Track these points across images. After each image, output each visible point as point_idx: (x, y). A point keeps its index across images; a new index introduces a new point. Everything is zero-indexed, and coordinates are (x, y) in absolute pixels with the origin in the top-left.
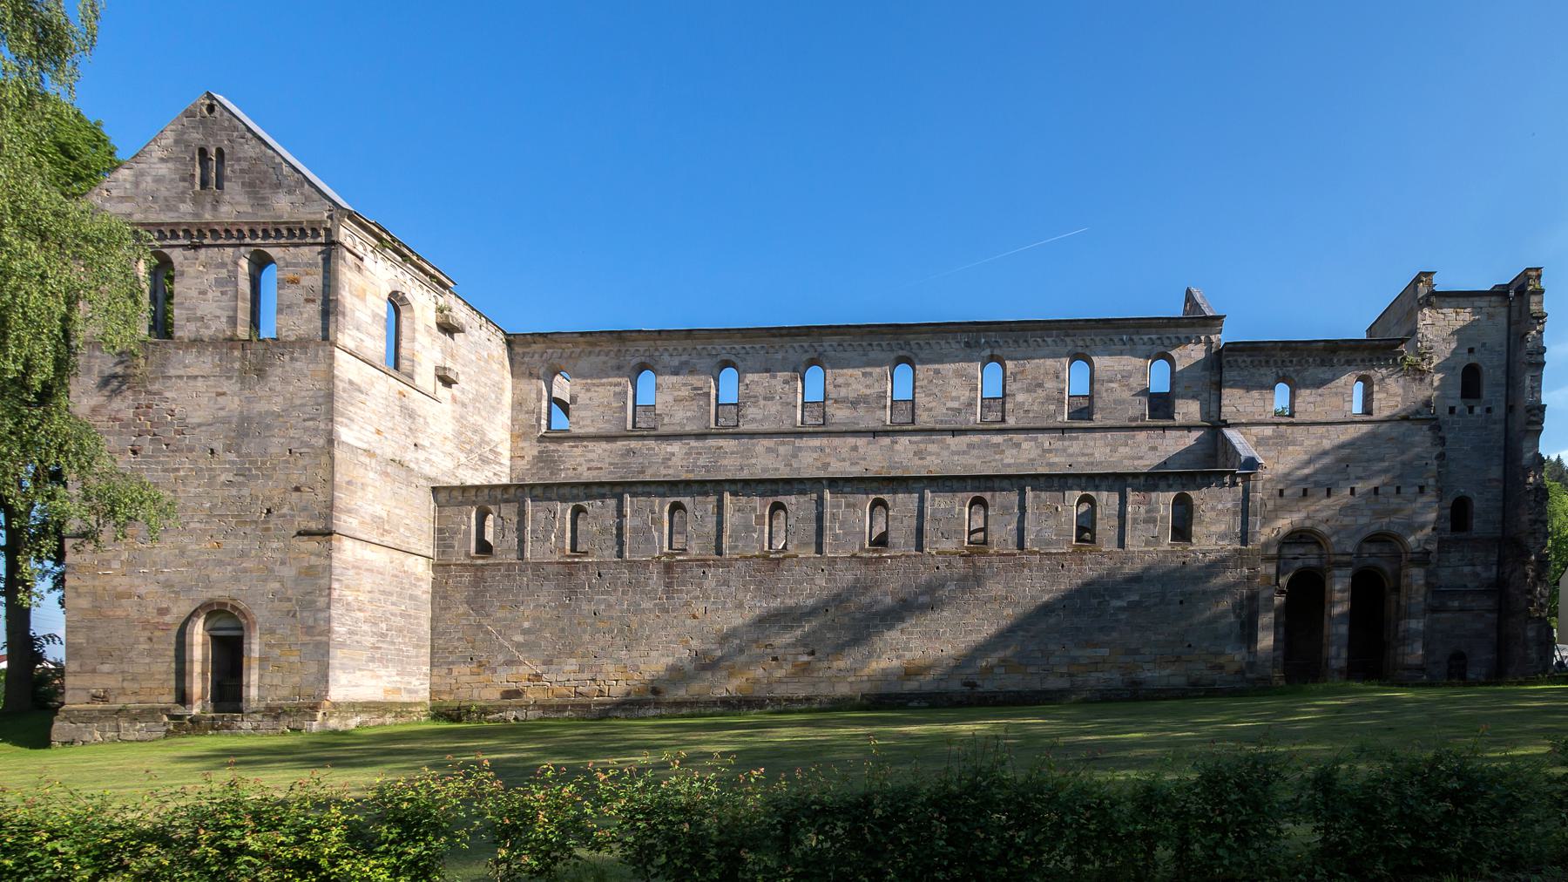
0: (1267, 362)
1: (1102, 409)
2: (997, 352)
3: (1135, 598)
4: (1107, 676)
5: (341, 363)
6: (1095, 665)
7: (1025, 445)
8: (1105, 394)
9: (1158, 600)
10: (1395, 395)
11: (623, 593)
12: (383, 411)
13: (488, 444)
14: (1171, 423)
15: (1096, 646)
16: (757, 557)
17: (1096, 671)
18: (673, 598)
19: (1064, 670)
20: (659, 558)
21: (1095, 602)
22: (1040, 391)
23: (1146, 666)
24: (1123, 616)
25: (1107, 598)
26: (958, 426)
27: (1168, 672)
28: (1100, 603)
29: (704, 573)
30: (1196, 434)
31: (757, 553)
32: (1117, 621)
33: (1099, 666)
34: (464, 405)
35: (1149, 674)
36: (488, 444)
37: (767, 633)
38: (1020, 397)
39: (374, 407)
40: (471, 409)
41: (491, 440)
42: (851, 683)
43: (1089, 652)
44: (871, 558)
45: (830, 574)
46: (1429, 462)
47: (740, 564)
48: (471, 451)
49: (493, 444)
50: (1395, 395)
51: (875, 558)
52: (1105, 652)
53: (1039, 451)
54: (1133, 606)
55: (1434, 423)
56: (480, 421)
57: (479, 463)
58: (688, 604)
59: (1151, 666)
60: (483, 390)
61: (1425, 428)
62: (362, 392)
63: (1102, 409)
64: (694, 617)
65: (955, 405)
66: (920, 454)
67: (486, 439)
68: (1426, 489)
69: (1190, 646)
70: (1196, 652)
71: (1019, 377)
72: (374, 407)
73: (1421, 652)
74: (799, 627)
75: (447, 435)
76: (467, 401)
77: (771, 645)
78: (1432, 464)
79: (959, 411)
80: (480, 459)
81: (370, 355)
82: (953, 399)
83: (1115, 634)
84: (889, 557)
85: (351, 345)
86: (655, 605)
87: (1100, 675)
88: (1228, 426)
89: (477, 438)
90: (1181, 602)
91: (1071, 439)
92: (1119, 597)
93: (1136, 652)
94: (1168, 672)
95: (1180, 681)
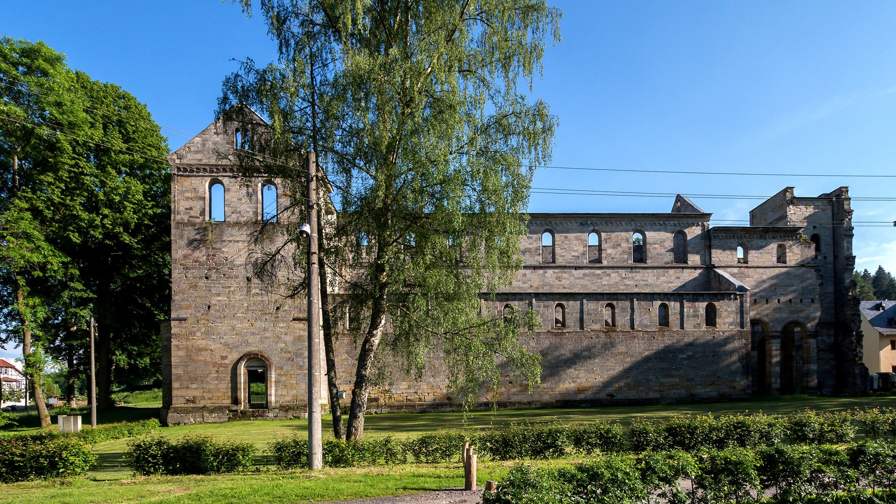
0: (734, 236)
1: (651, 258)
2: (596, 228)
3: (690, 353)
4: (678, 391)
7: (613, 275)
8: (652, 250)
14: (686, 265)
15: (672, 377)
19: (657, 388)
21: (671, 355)
22: (619, 248)
23: (697, 387)
24: (685, 362)
26: (578, 265)
30: (699, 271)
38: (609, 251)
43: (669, 380)
52: (677, 380)
53: (620, 278)
59: (700, 387)
63: (651, 258)
65: (576, 254)
66: (559, 279)
71: (608, 241)
73: (816, 381)
79: (578, 257)
82: (575, 251)
83: (682, 372)
87: (675, 391)
88: (716, 267)
91: (636, 272)
92: (683, 353)
93: (692, 380)
95: (714, 394)
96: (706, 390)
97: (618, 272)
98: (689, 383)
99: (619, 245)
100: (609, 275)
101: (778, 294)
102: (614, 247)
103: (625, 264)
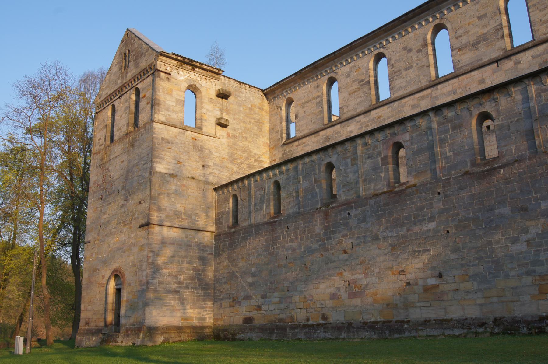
5: (157, 129)
11: (301, 240)
12: (182, 150)
13: (253, 157)
16: (385, 193)
18: (330, 238)
20: (320, 208)
29: (349, 214)
31: (385, 190)
34: (235, 137)
36: (253, 157)
37: (399, 260)
39: (177, 149)
40: (240, 139)
41: (255, 154)
42: (481, 305)
44: (483, 172)
45: (446, 196)
47: (373, 201)
48: (241, 163)
49: (257, 156)
51: (488, 170)
56: (246, 144)
57: (247, 169)
58: (340, 242)
60: (248, 126)
62: (169, 143)
64: (345, 252)
67: (252, 154)
72: (177, 149)
74: (425, 251)
75: (224, 156)
76: (238, 135)
77: (403, 271)
80: (248, 167)
81: (197, 124)
84: (500, 167)
85: (162, 118)
86: (320, 246)
89: (245, 155)
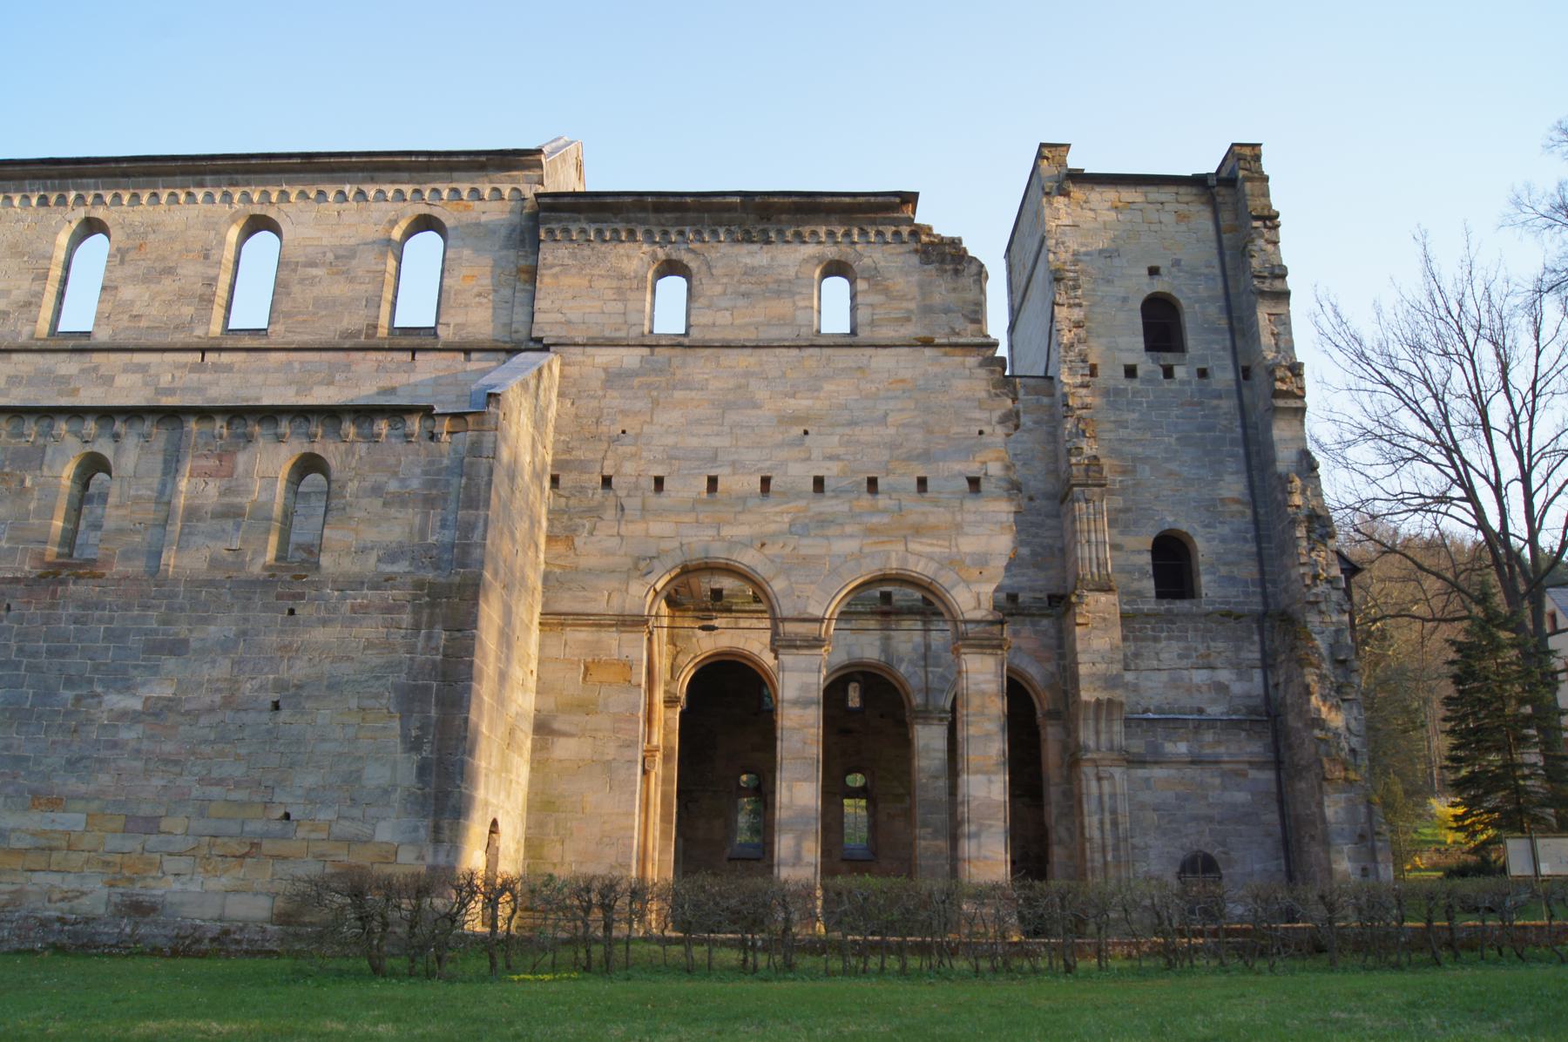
3: (167, 691)
4: (71, 883)
6: (45, 849)
9: (218, 698)
10: (903, 298)
15: (55, 803)
17: (48, 870)
21: (68, 695)
23: (171, 865)
24: (128, 734)
25: (99, 690)
27: (225, 881)
28: (78, 699)
32: (114, 745)
33: (56, 856)
35: (176, 886)
43: (36, 820)
46: (987, 429)
50: (903, 298)
54: (156, 712)
55: (989, 352)
59: (182, 864)
61: (972, 360)
68: (984, 485)
69: (287, 816)
70: (301, 833)
78: (993, 434)
83: (105, 779)
87: (55, 879)
90: (276, 706)
93: (151, 825)
94: (225, 881)
96: (214, 884)
97: (143, 369)
98: (133, 844)
99: (169, 271)
100: (108, 381)
101: (816, 454)
102: (146, 279)
103: (179, 338)
